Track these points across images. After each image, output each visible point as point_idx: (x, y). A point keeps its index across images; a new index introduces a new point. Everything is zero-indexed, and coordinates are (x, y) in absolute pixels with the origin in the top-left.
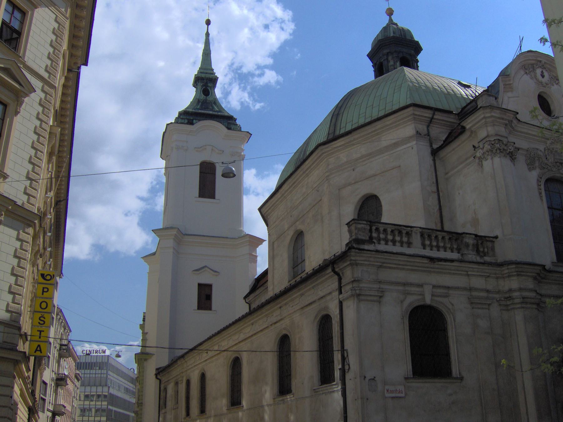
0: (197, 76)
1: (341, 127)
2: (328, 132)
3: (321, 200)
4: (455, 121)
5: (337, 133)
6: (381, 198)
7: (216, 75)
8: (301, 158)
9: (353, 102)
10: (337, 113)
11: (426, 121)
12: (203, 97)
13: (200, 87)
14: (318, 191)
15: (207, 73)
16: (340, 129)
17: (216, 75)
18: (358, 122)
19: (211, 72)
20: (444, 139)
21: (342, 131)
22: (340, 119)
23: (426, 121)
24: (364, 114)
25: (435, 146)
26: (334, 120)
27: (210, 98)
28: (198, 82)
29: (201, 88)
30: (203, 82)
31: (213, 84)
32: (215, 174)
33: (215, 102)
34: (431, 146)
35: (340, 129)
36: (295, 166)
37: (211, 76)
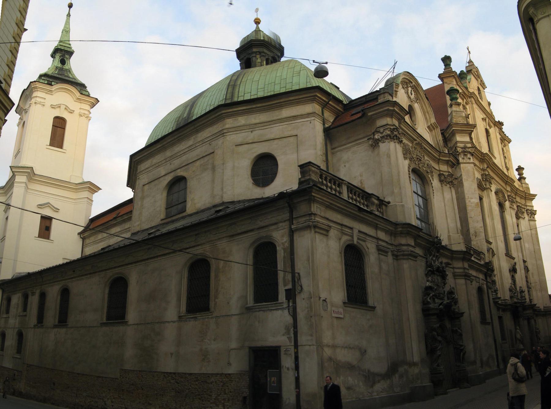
0: (56, 48)
1: (239, 96)
2: (224, 97)
3: (214, 152)
4: (342, 110)
5: (236, 99)
6: (278, 159)
7: (72, 49)
8: (186, 117)
9: (249, 78)
10: (233, 84)
11: (322, 104)
12: (60, 65)
13: (59, 57)
14: (210, 145)
15: (65, 46)
16: (238, 97)
17: (72, 49)
18: (257, 94)
19: (69, 46)
20: (332, 121)
21: (241, 99)
22: (237, 90)
23: (322, 104)
24: (263, 89)
25: (327, 126)
26: (230, 89)
27: (66, 67)
28: (57, 53)
29: (59, 58)
30: (61, 53)
31: (69, 56)
32: (64, 129)
33: (69, 71)
34: (324, 124)
35: (238, 97)
36: (176, 123)
37: (69, 50)
